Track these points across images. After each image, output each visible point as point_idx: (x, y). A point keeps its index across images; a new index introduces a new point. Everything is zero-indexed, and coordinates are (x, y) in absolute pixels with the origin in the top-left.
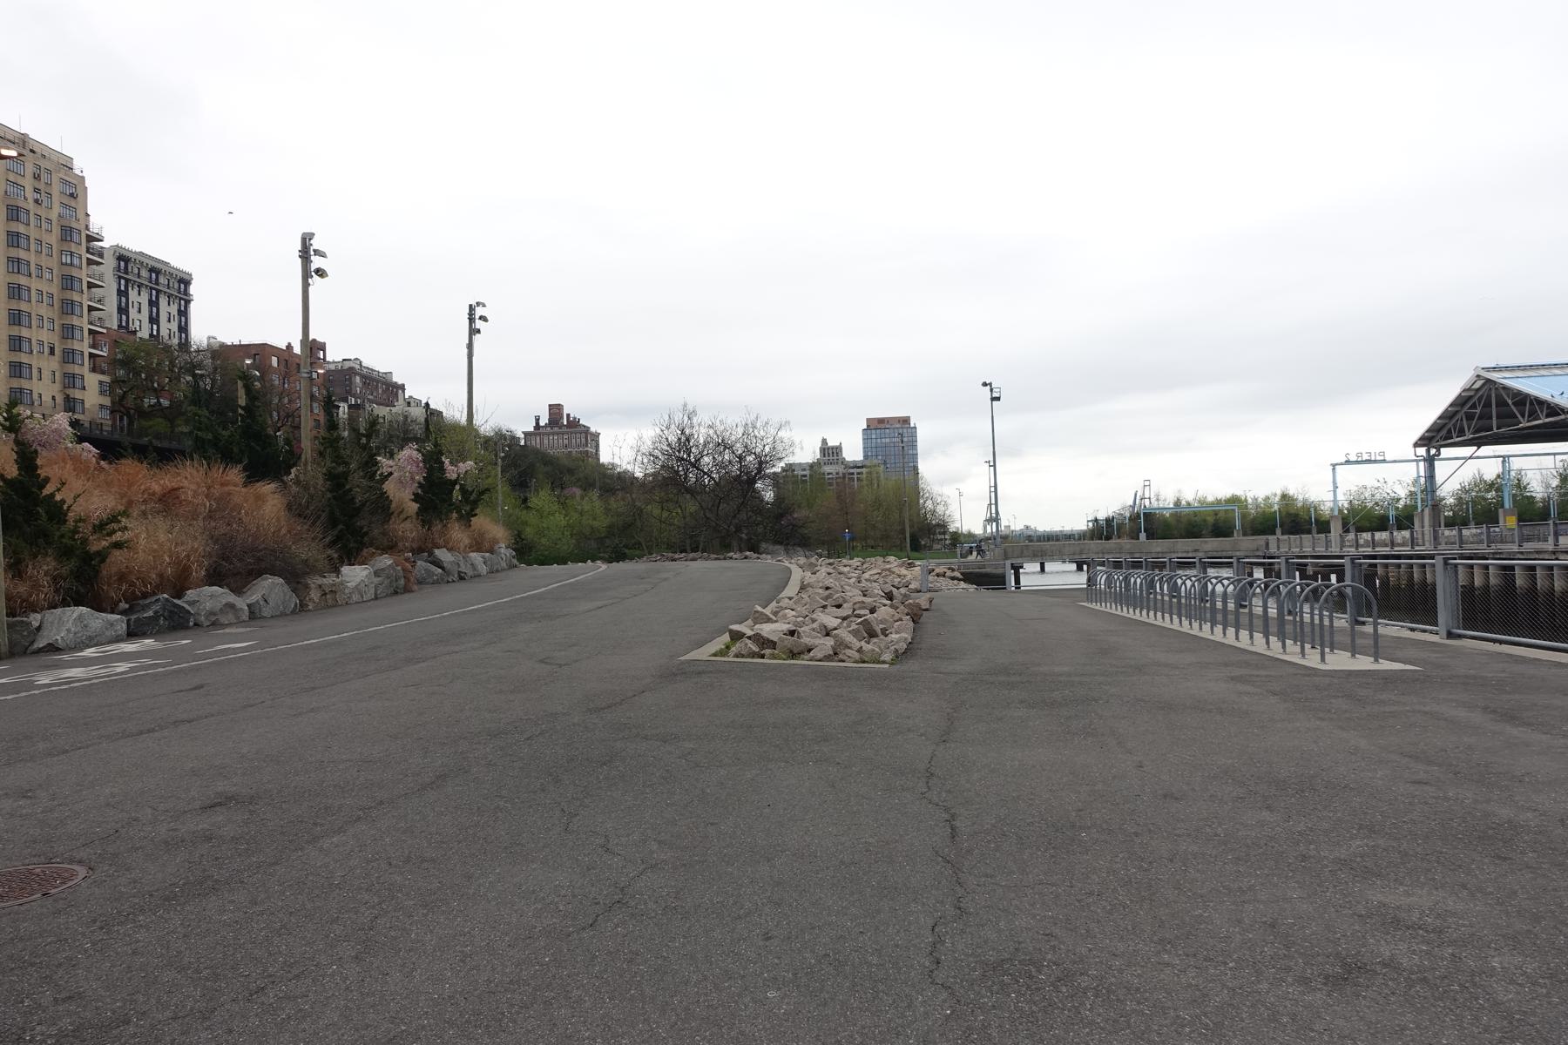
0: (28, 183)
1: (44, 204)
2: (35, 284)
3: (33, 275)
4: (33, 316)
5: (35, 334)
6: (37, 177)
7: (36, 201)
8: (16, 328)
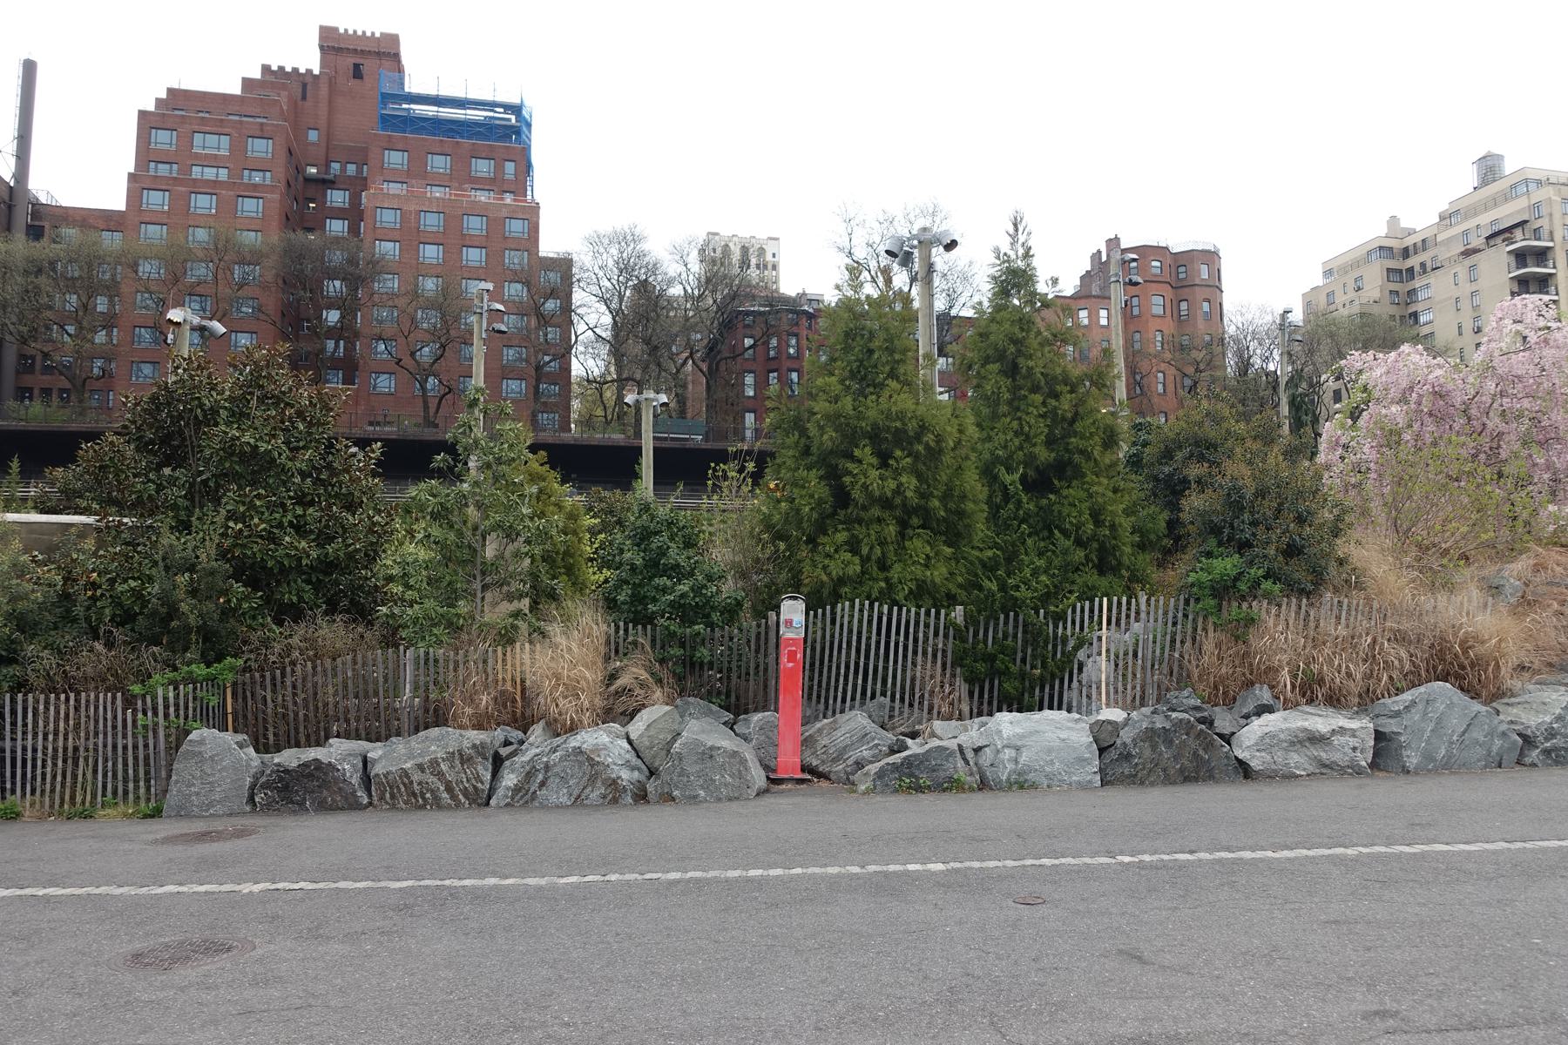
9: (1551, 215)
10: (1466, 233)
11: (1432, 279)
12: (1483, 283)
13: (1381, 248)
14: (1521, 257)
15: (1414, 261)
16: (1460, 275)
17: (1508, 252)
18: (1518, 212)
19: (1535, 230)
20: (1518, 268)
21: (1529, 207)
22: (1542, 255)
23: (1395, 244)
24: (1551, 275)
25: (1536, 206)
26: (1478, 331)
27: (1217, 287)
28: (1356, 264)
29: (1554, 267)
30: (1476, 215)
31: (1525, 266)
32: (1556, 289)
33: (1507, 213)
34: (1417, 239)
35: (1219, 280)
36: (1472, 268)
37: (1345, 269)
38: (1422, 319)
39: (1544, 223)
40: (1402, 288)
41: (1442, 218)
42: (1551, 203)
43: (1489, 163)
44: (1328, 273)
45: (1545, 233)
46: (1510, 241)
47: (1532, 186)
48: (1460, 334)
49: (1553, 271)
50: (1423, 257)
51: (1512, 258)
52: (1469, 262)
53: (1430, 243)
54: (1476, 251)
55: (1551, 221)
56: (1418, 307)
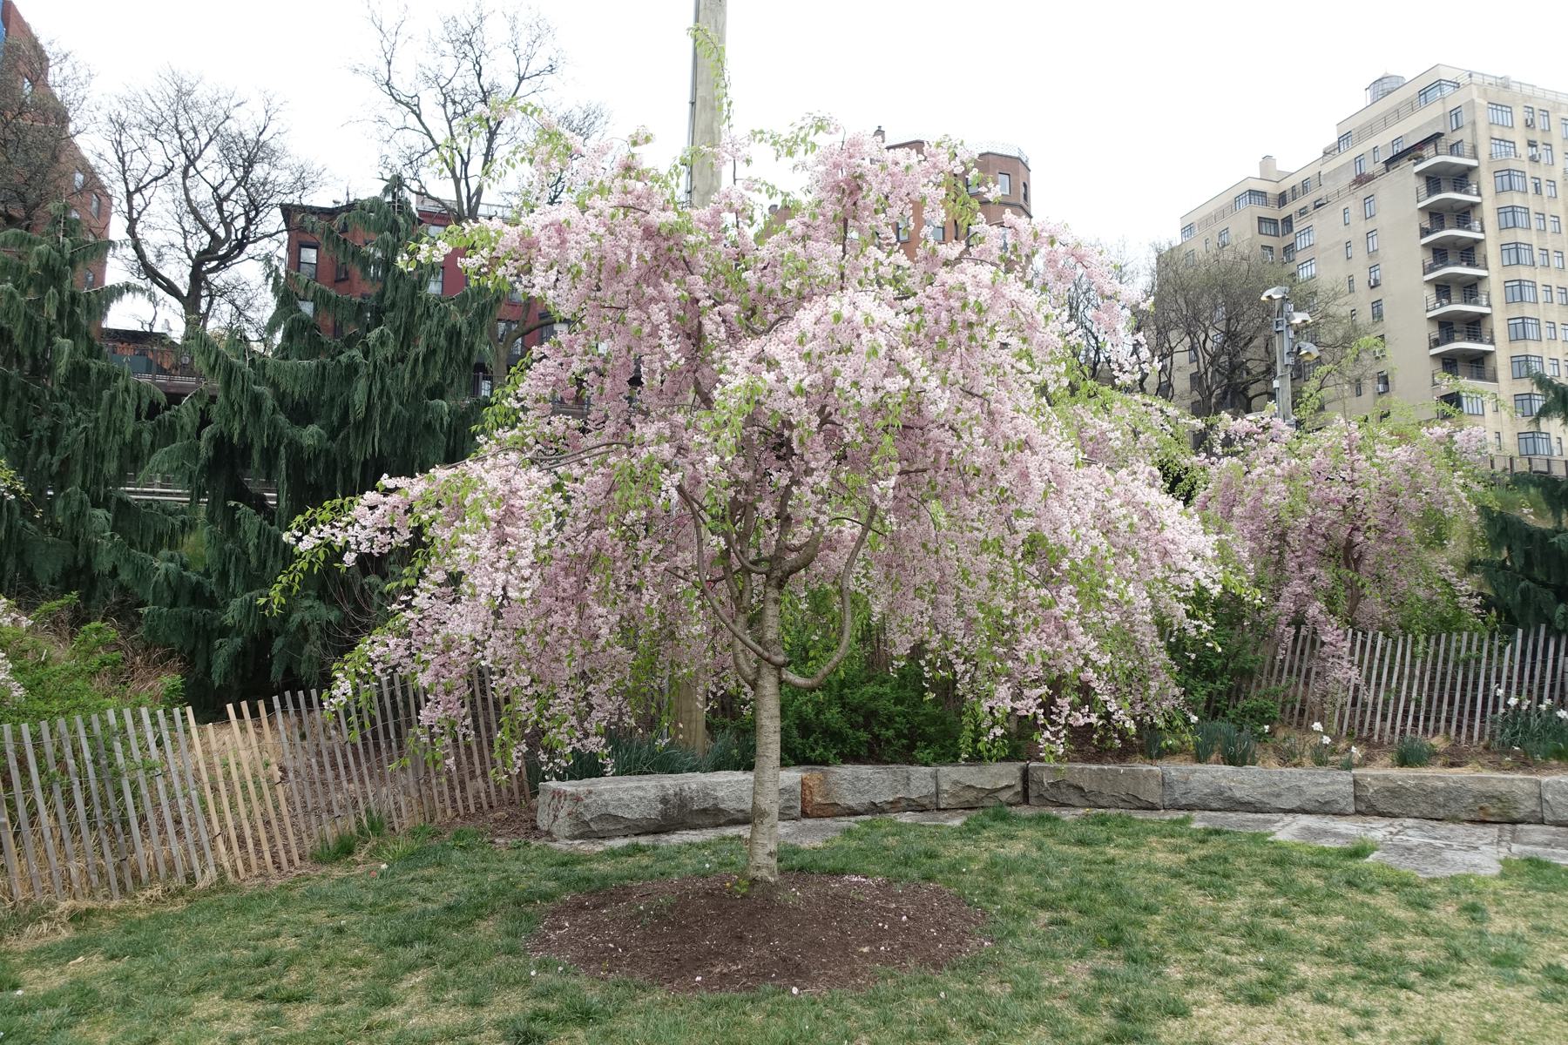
0: (1519, 136)
1: (1543, 161)
2: (1541, 278)
3: (1537, 265)
4: (1543, 325)
5: (1545, 351)
6: (1529, 125)
7: (1533, 159)
8: (1521, 344)
9: (1474, 123)
10: (1358, 160)
11: (1316, 220)
12: (1382, 220)
13: (1251, 192)
14: (1434, 180)
15: (1290, 209)
16: (1351, 211)
17: (1417, 174)
18: (1429, 123)
19: (1452, 146)
20: (1429, 196)
21: (1444, 115)
22: (1462, 178)
23: (1271, 189)
24: (1474, 205)
25: (1455, 113)
26: (1375, 285)
27: (1021, 207)
28: (1221, 214)
29: (1479, 194)
30: (1372, 134)
31: (1439, 191)
32: (1482, 224)
33: (1412, 128)
34: (1296, 181)
35: (1026, 197)
36: (1368, 199)
37: (1207, 221)
38: (1304, 274)
39: (1464, 135)
40: (1278, 243)
41: (1325, 154)
42: (1474, 107)
43: (1385, 86)
44: (1187, 229)
45: (1467, 149)
46: (1420, 159)
47: (1448, 90)
48: (1351, 291)
49: (1477, 199)
50: (1306, 201)
51: (1421, 184)
52: (1362, 192)
53: (1314, 183)
54: (1370, 178)
55: (1474, 130)
56: (1300, 257)
